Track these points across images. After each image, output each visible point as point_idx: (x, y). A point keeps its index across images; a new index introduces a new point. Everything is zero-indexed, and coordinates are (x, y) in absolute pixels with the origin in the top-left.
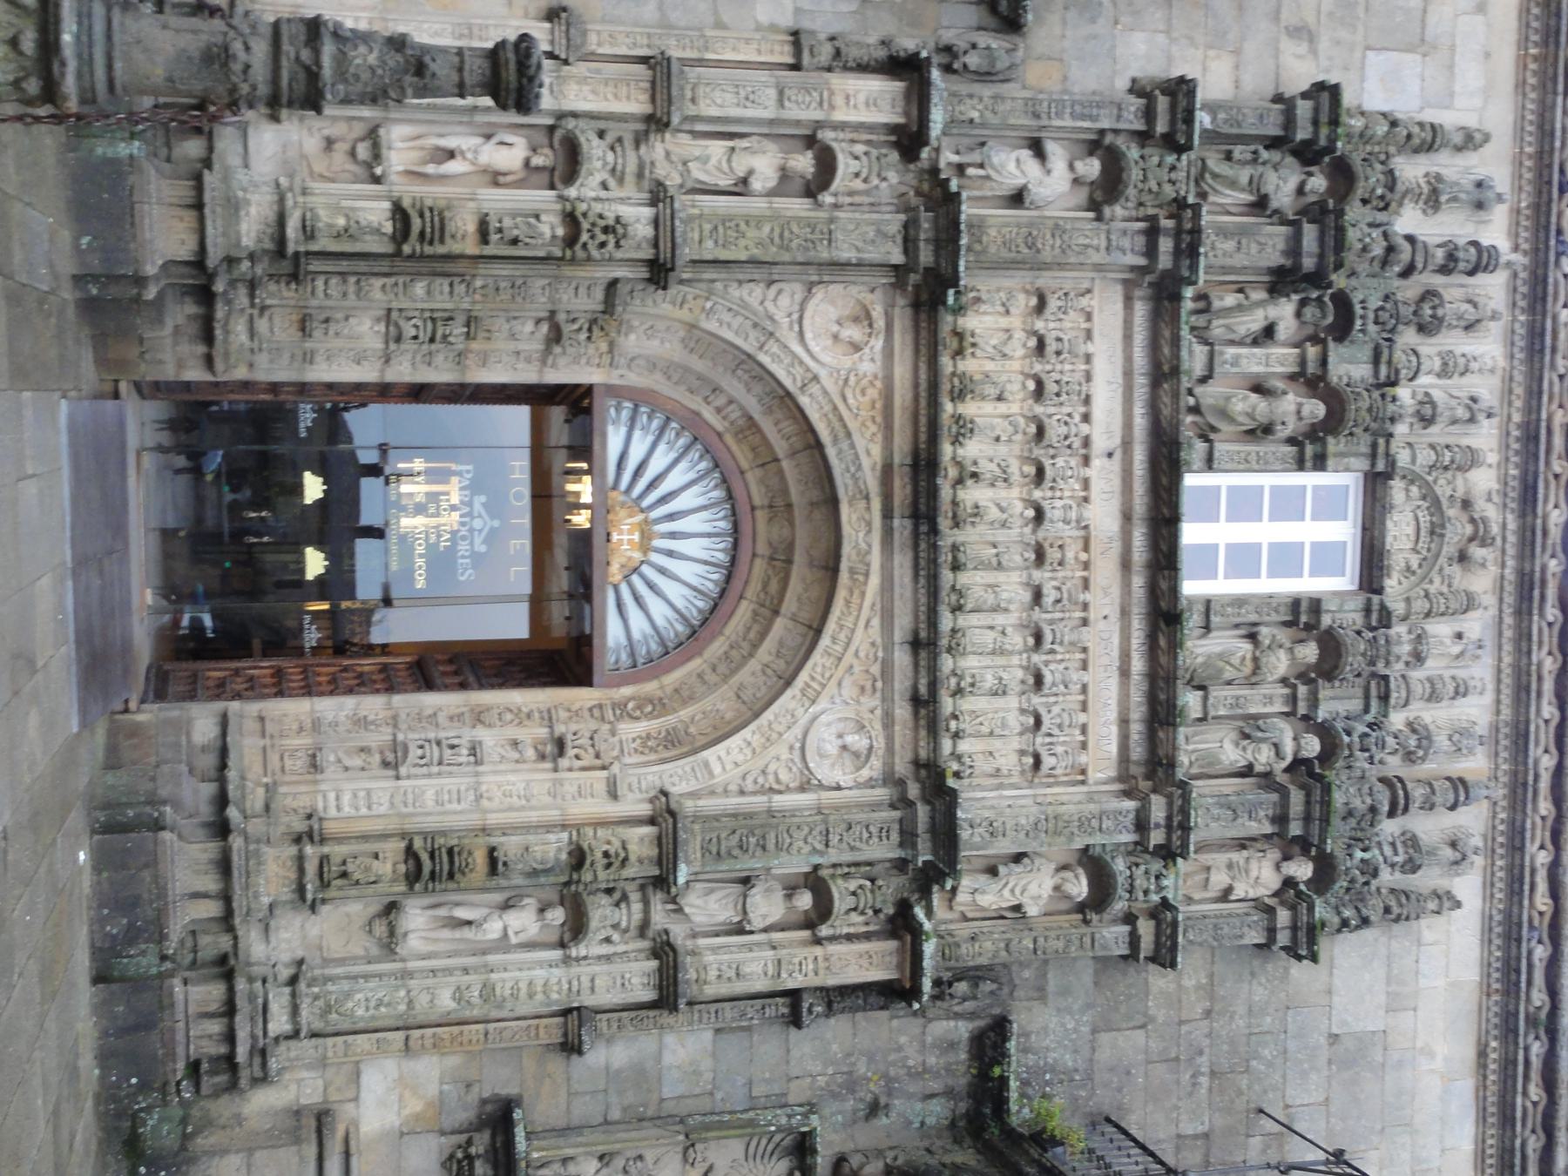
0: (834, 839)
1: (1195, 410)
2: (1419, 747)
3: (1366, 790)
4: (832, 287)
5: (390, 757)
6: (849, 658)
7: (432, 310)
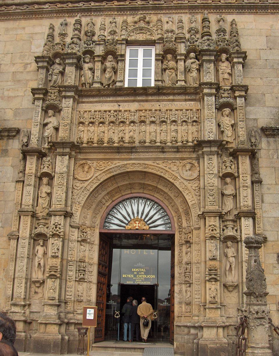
0: (211, 172)
1: (109, 85)
2: (194, 30)
3: (204, 42)
4: (75, 174)
5: (188, 285)
6: (167, 169)
7: (76, 270)
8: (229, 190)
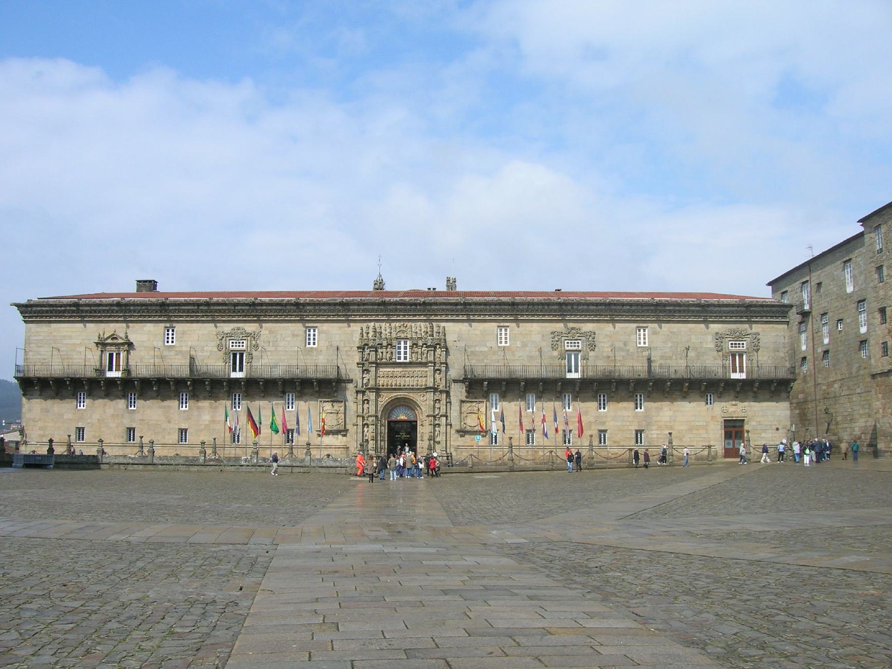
8: (437, 405)
